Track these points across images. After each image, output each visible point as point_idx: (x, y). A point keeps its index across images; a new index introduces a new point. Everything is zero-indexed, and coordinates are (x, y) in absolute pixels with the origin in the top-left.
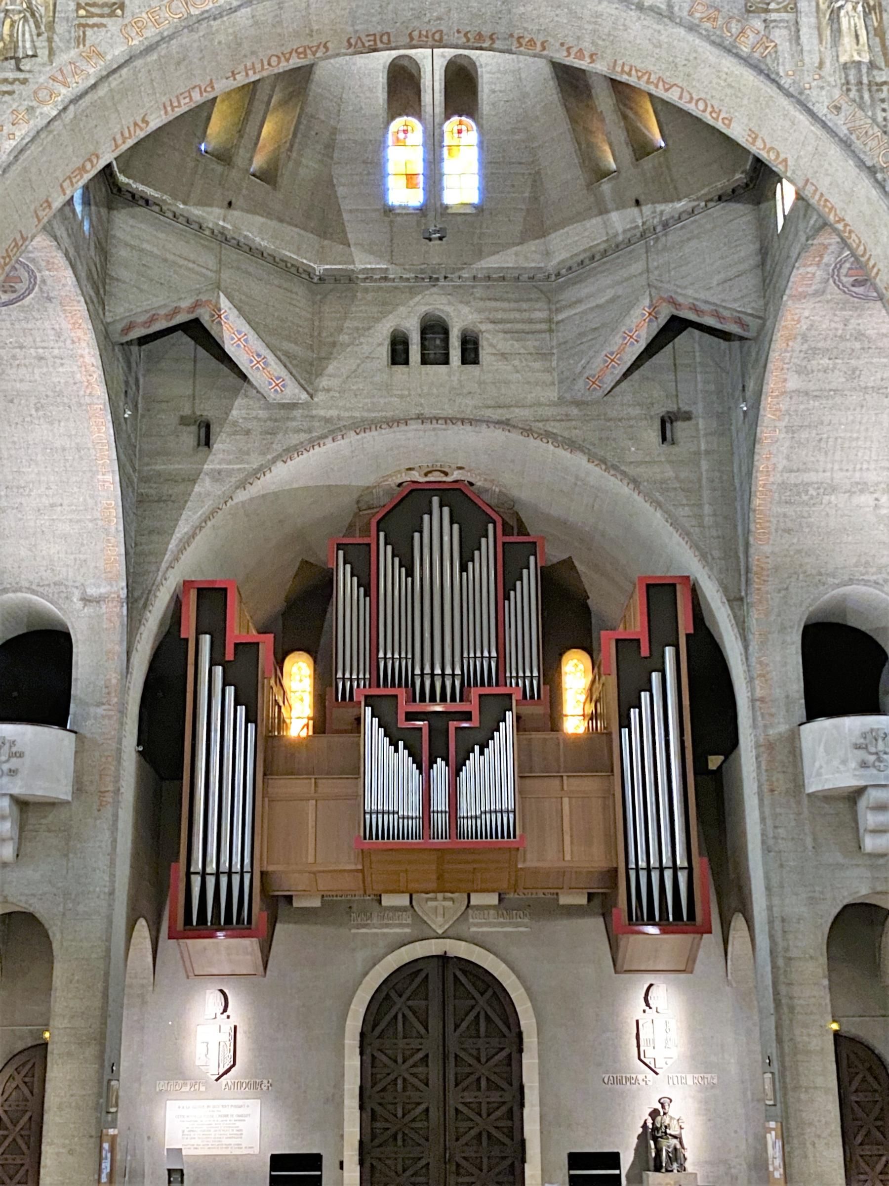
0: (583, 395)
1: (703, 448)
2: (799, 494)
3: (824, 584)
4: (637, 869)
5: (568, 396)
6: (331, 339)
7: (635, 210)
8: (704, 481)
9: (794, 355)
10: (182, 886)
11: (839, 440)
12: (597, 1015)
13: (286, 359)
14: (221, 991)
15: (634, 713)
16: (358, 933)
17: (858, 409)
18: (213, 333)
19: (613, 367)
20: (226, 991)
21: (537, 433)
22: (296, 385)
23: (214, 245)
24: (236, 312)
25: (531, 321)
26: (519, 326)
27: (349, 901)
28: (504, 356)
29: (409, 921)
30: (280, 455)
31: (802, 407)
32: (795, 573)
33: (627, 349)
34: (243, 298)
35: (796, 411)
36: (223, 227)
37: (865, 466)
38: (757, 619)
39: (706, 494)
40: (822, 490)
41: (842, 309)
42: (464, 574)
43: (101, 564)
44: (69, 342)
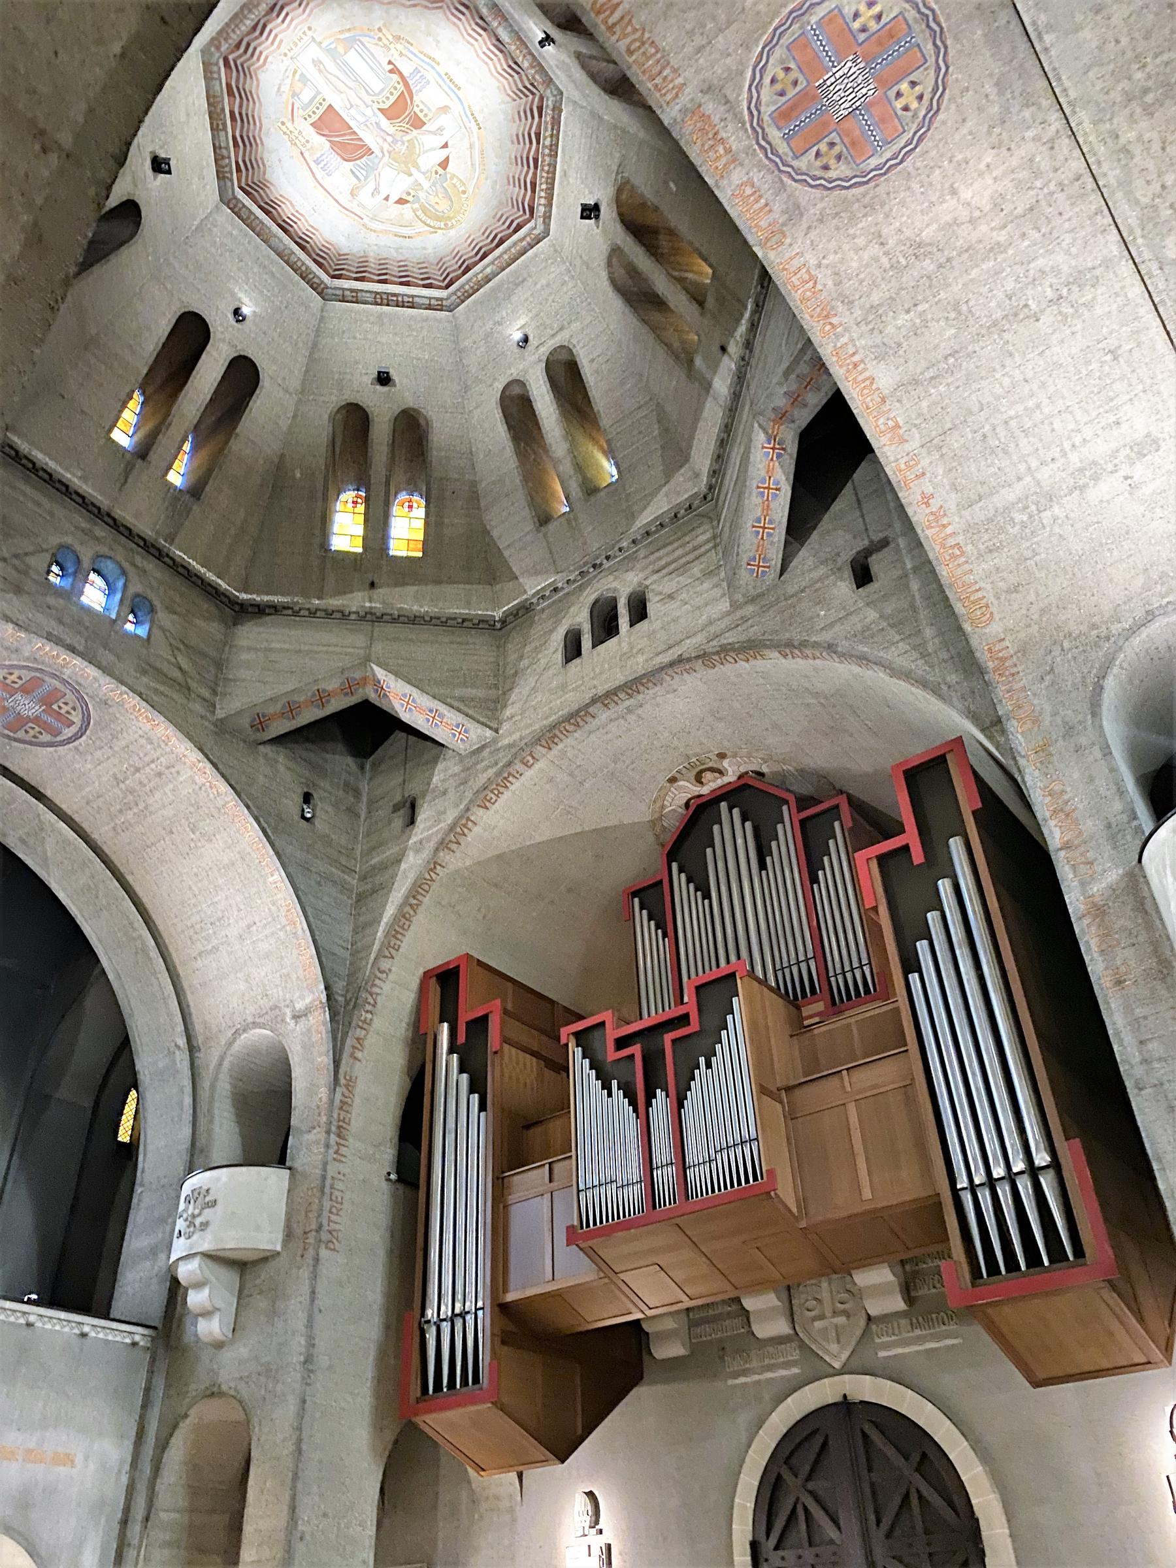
0: (754, 588)
1: (909, 566)
2: (1002, 530)
3: (1108, 638)
4: (973, 1188)
5: (739, 597)
6: (512, 672)
7: (726, 358)
8: (918, 602)
9: (855, 336)
10: (417, 1339)
11: (1013, 423)
12: (1098, 1475)
13: (460, 705)
14: (591, 1495)
15: (922, 946)
16: (736, 1386)
17: (1008, 362)
18: (385, 708)
19: (769, 535)
20: (596, 1493)
21: (714, 654)
22: (477, 725)
23: (367, 627)
24: (393, 677)
25: (695, 549)
26: (684, 560)
27: (721, 1340)
28: (671, 597)
29: (796, 1355)
30: (471, 801)
31: (924, 404)
32: (1055, 643)
33: (772, 505)
34: (400, 662)
35: (919, 415)
36: (371, 608)
37: (1078, 440)
38: (1022, 733)
39: (923, 614)
40: (1033, 508)
41: (853, 219)
42: (764, 873)
43: (301, 973)
44: (163, 745)
